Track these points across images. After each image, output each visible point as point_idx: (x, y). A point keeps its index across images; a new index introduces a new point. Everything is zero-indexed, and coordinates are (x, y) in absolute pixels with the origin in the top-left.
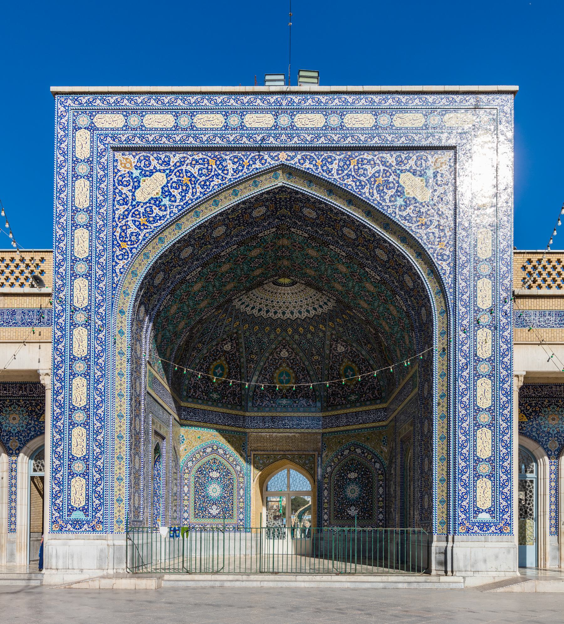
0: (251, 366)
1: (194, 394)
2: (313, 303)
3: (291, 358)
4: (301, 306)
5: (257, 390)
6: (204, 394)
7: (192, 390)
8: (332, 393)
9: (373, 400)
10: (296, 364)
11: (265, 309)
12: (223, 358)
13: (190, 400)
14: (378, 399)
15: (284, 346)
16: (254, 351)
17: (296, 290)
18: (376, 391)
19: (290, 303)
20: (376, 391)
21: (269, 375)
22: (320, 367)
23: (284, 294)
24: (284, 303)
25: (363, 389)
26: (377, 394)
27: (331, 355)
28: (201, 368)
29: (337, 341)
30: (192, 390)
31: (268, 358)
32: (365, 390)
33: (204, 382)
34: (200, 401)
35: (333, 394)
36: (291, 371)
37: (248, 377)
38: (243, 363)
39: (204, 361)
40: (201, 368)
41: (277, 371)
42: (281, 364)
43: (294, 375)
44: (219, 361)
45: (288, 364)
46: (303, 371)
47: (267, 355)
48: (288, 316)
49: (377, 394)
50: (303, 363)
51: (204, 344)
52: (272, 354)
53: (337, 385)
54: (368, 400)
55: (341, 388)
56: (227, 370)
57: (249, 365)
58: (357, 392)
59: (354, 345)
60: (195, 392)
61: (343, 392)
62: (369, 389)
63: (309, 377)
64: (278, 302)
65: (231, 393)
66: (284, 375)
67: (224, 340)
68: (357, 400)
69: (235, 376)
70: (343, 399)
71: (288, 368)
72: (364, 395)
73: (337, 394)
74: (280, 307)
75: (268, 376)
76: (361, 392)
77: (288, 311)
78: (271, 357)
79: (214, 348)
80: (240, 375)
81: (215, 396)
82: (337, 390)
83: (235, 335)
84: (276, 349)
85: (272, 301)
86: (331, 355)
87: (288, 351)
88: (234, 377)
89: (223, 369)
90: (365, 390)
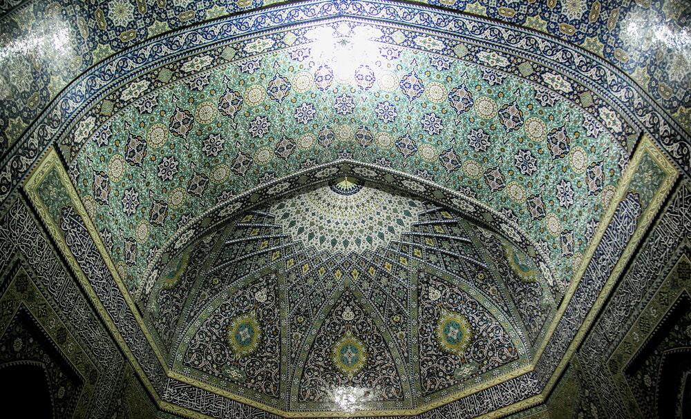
0: (297, 335)
1: (196, 363)
2: (389, 218)
3: (359, 321)
4: (371, 228)
5: (306, 375)
6: (215, 366)
7: (195, 355)
8: (429, 372)
9: (503, 364)
10: (366, 332)
11: (319, 235)
12: (253, 314)
13: (187, 370)
14: (513, 360)
15: (348, 302)
16: (303, 310)
17: (363, 199)
18: (506, 350)
19: (355, 224)
20: (506, 350)
21: (326, 351)
22: (404, 333)
23: (346, 208)
24: (346, 224)
25: (481, 352)
26: (509, 354)
27: (420, 309)
28: (216, 323)
29: (427, 283)
30: (195, 355)
31: (324, 322)
32: (485, 353)
33: (218, 347)
34: (205, 377)
35: (430, 375)
36: (360, 343)
37: (292, 353)
38: (285, 328)
39: (222, 311)
40: (216, 323)
41: (338, 344)
42: (343, 332)
43: (364, 349)
44: (246, 317)
45: (354, 332)
46: (379, 343)
47: (323, 317)
48: (353, 248)
49: (509, 354)
50: (377, 329)
51: (223, 281)
52: (329, 315)
53: (434, 358)
54: (494, 368)
55: (442, 362)
56: (259, 336)
57: (294, 334)
58: (471, 360)
59: (455, 282)
60: (200, 360)
61: (447, 366)
62: (493, 350)
63: (389, 351)
64: (337, 223)
65: (262, 375)
66: (349, 350)
67: (256, 281)
68: (474, 375)
69: (272, 348)
70: (448, 377)
71: (354, 339)
72: (485, 362)
73: (438, 372)
74: (341, 233)
75: (323, 353)
76: (479, 358)
77: (352, 240)
78: (328, 321)
79: (240, 292)
80: (280, 348)
81: (234, 373)
82: (436, 365)
83: (273, 276)
84: (335, 306)
85: (329, 221)
86: (420, 309)
87: (353, 310)
88: (269, 349)
89: (251, 332)
90: (485, 353)
